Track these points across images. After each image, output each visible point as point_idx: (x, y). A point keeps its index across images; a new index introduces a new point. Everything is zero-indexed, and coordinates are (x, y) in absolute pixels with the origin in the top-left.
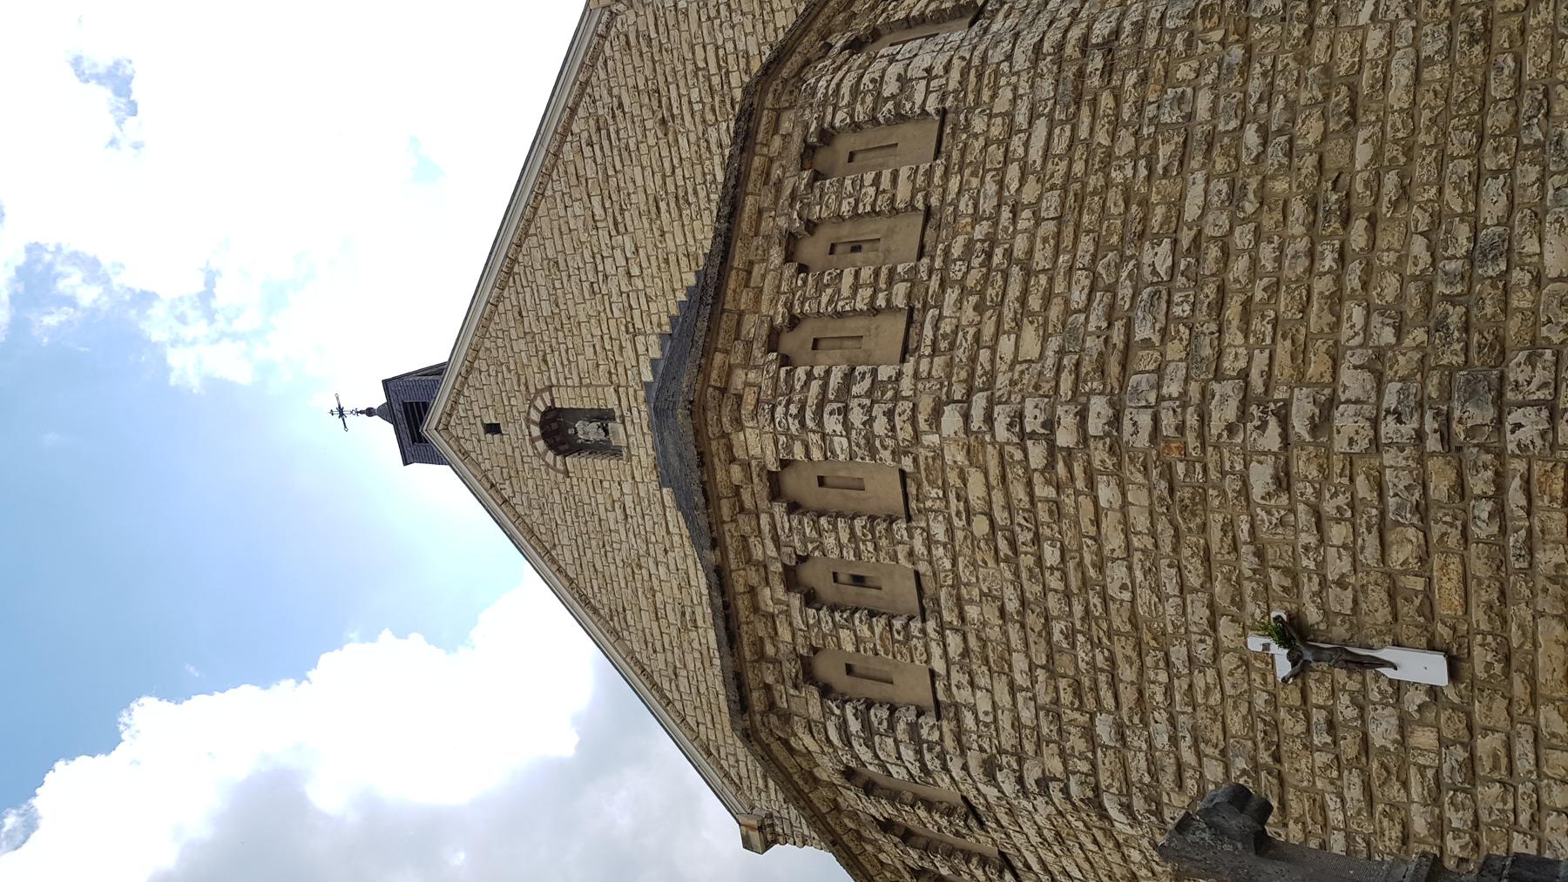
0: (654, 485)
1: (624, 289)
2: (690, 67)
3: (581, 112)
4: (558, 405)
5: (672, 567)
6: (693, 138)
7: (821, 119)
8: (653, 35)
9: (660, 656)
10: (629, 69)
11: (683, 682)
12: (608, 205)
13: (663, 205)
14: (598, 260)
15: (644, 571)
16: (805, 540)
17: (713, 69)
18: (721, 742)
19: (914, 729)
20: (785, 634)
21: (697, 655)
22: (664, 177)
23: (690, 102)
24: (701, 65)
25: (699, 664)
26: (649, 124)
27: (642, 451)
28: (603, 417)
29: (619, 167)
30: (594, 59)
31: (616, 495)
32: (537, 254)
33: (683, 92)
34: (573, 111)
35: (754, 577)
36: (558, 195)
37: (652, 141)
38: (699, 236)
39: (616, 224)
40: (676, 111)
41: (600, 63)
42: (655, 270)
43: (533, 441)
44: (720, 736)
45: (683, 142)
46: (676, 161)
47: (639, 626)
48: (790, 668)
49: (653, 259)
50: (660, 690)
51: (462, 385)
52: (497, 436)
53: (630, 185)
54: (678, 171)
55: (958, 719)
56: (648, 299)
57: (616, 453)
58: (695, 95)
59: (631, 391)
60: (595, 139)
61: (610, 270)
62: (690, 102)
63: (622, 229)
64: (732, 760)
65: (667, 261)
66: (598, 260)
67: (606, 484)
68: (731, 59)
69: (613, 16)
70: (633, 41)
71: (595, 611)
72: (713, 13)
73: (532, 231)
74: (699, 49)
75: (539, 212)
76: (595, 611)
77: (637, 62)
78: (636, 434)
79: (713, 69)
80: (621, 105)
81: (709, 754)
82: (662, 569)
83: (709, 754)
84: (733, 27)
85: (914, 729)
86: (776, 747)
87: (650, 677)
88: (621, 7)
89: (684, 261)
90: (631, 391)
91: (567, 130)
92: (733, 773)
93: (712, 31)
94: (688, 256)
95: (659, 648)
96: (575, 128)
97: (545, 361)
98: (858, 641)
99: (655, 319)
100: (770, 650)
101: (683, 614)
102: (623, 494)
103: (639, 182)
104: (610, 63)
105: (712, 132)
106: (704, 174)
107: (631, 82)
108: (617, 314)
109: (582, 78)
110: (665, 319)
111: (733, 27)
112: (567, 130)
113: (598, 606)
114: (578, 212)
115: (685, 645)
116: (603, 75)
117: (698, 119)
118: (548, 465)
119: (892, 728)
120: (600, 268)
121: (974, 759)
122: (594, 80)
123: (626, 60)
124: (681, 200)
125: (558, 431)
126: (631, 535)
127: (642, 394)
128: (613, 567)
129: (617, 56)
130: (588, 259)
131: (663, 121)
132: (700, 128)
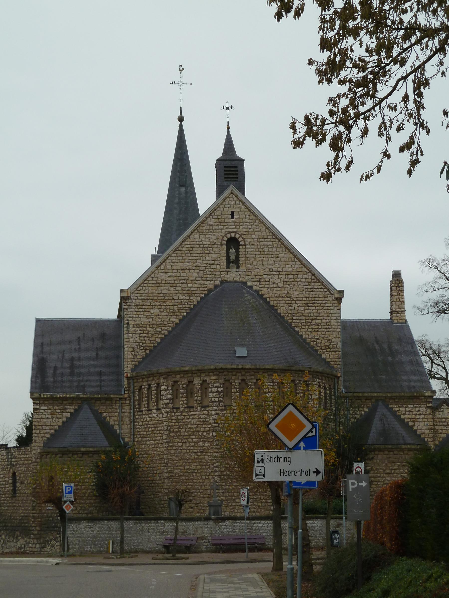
0: (220, 279)
1: (271, 280)
2: (318, 315)
3: (313, 277)
4: (241, 247)
5: (197, 279)
6: (303, 312)
7: (310, 384)
8: (326, 305)
9: (170, 267)
10: (320, 296)
11: (164, 275)
12: (291, 280)
13: (289, 299)
14: (278, 273)
15: (194, 268)
16: (251, 385)
17: (317, 321)
18: (149, 285)
19: (221, 401)
20: (233, 378)
21: (173, 282)
22: (295, 301)
23: (310, 313)
24: (318, 318)
25: (171, 282)
26: (307, 299)
27: (228, 276)
28: (237, 261)
29: (300, 286)
30: (324, 286)
31: (216, 262)
32: (280, 250)
33: (313, 311)
34: (314, 275)
35: (243, 373)
36: (294, 263)
37: (304, 299)
38: (282, 308)
39: (286, 282)
40: (309, 308)
41: (322, 286)
42: (275, 292)
43: (230, 233)
44: (151, 285)
45: (303, 308)
46: (298, 305)
47: (178, 261)
48: (227, 378)
49: (277, 292)
50: (160, 265)
51: (245, 206)
52: (230, 216)
53: (294, 289)
54: (296, 305)
55: (225, 410)
56: (268, 288)
57: (228, 267)
58: (312, 315)
59: (244, 276)
60: (307, 280)
61: (276, 277)
62: (310, 313)
63: (285, 283)
64: (144, 288)
65: (276, 297)
66: (278, 273)
67: (219, 259)
68: (317, 327)
69: (332, 294)
70: (326, 299)
71: (181, 244)
72: (327, 324)
73: (287, 250)
74: (320, 318)
75: (291, 254)
76: (181, 244)
77: (322, 299)
78: (232, 275)
79: (317, 321)
80: (313, 291)
81: (145, 280)
82: (196, 275)
83: (145, 280)
84: (324, 329)
85: (221, 401)
86: (211, 371)
87: (164, 262)
88: (333, 298)
89: (276, 302)
90: (244, 276)
91: (310, 272)
92: (140, 288)
93: (324, 323)
94: (277, 304)
95: (173, 267)
96: (310, 274)
97: (252, 245)
98: (235, 393)
99: (263, 289)
100: (230, 374)
101: (184, 280)
102: (217, 265)
103: (296, 292)
104: (322, 290)
105: (303, 318)
106: (295, 313)
107: (317, 295)
108: (265, 276)
109: (320, 281)
110: (263, 292)
111: (324, 329)
112: (310, 272)
113: (182, 246)
114: (291, 269)
115: (175, 278)
116: (320, 287)
117: (307, 315)
118: (223, 237)
119: (221, 397)
120: (276, 273)
121: (218, 412)
122: (319, 284)
123: (322, 295)
124: (290, 305)
125: (233, 243)
126: (205, 265)
127: (244, 280)
128: (195, 255)
129: (323, 293)
130: (279, 270)
131: (308, 304)
132: (305, 315)
